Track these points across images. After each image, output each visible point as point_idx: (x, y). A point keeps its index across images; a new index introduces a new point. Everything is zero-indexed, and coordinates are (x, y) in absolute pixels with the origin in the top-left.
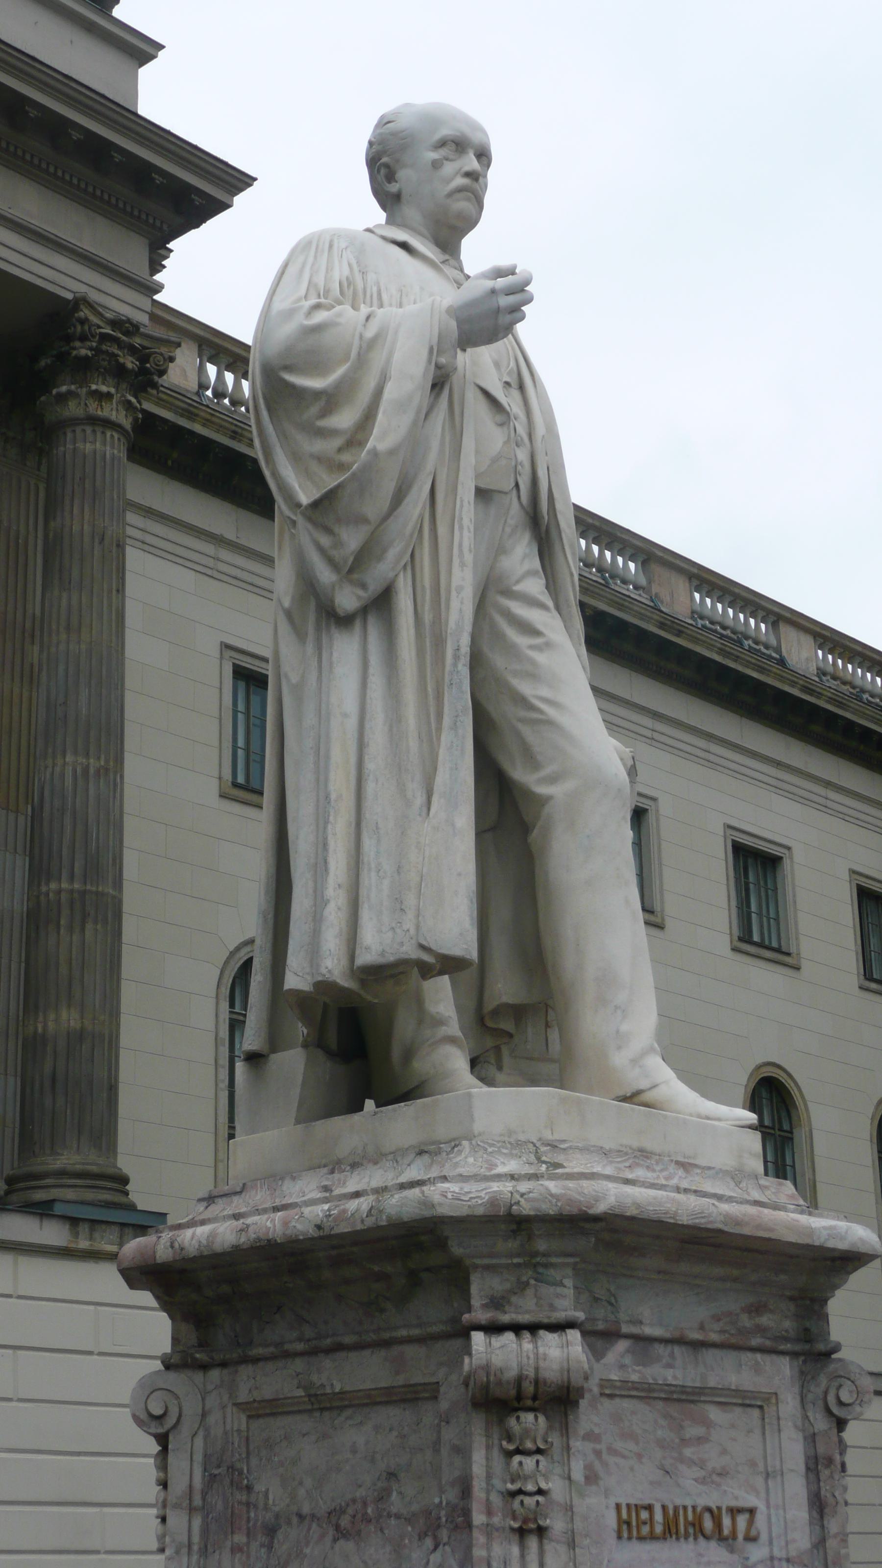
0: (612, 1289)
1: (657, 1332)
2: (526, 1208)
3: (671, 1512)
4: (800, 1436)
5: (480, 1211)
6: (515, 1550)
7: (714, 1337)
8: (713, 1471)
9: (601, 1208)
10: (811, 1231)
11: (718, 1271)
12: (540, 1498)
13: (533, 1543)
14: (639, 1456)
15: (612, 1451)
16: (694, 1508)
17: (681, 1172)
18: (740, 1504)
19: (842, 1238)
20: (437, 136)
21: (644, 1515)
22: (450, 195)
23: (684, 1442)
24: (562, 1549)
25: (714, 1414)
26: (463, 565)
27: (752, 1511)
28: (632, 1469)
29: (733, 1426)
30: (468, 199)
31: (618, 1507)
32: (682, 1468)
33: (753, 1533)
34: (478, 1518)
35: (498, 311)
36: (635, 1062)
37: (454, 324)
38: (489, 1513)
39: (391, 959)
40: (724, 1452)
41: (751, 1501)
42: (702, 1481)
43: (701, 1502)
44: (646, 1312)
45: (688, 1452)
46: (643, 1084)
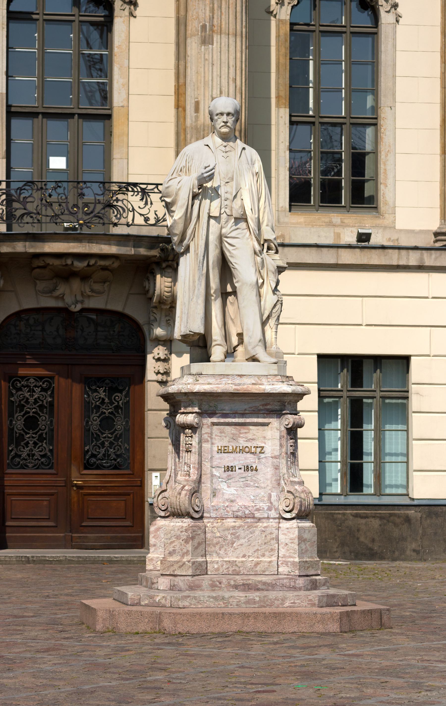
0: (216, 404)
1: (228, 412)
2: (183, 391)
3: (235, 448)
4: (279, 431)
5: (176, 392)
6: (186, 455)
7: (247, 412)
8: (250, 439)
9: (195, 391)
10: (265, 390)
11: (247, 398)
12: (189, 445)
13: (189, 453)
14: (226, 437)
15: (216, 435)
16: (243, 447)
17: (239, 378)
18: (259, 446)
19: (276, 390)
20: (216, 113)
21: (225, 448)
22: (220, 128)
23: (240, 433)
24: (194, 454)
25: (251, 427)
26: (202, 239)
27: (263, 448)
28: (223, 439)
29: (258, 430)
30: (225, 128)
31: (218, 447)
32: (240, 439)
33: (263, 451)
34: (181, 449)
35: (205, 178)
36: (253, 348)
37: (196, 182)
38: (183, 448)
39: (185, 334)
40: (254, 435)
41: (263, 445)
42: (246, 441)
43: (245, 445)
44: (227, 408)
45: (242, 435)
46: (255, 354)
